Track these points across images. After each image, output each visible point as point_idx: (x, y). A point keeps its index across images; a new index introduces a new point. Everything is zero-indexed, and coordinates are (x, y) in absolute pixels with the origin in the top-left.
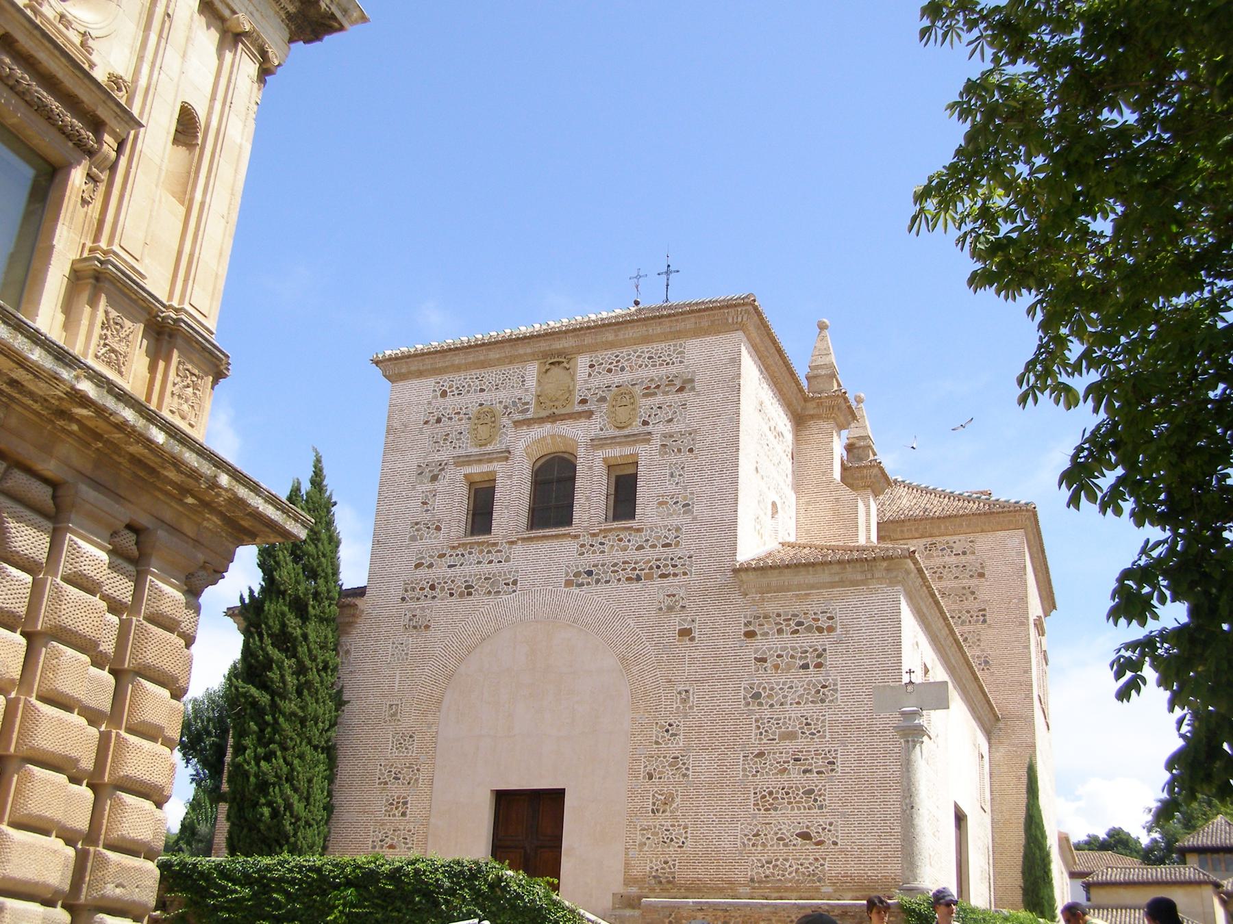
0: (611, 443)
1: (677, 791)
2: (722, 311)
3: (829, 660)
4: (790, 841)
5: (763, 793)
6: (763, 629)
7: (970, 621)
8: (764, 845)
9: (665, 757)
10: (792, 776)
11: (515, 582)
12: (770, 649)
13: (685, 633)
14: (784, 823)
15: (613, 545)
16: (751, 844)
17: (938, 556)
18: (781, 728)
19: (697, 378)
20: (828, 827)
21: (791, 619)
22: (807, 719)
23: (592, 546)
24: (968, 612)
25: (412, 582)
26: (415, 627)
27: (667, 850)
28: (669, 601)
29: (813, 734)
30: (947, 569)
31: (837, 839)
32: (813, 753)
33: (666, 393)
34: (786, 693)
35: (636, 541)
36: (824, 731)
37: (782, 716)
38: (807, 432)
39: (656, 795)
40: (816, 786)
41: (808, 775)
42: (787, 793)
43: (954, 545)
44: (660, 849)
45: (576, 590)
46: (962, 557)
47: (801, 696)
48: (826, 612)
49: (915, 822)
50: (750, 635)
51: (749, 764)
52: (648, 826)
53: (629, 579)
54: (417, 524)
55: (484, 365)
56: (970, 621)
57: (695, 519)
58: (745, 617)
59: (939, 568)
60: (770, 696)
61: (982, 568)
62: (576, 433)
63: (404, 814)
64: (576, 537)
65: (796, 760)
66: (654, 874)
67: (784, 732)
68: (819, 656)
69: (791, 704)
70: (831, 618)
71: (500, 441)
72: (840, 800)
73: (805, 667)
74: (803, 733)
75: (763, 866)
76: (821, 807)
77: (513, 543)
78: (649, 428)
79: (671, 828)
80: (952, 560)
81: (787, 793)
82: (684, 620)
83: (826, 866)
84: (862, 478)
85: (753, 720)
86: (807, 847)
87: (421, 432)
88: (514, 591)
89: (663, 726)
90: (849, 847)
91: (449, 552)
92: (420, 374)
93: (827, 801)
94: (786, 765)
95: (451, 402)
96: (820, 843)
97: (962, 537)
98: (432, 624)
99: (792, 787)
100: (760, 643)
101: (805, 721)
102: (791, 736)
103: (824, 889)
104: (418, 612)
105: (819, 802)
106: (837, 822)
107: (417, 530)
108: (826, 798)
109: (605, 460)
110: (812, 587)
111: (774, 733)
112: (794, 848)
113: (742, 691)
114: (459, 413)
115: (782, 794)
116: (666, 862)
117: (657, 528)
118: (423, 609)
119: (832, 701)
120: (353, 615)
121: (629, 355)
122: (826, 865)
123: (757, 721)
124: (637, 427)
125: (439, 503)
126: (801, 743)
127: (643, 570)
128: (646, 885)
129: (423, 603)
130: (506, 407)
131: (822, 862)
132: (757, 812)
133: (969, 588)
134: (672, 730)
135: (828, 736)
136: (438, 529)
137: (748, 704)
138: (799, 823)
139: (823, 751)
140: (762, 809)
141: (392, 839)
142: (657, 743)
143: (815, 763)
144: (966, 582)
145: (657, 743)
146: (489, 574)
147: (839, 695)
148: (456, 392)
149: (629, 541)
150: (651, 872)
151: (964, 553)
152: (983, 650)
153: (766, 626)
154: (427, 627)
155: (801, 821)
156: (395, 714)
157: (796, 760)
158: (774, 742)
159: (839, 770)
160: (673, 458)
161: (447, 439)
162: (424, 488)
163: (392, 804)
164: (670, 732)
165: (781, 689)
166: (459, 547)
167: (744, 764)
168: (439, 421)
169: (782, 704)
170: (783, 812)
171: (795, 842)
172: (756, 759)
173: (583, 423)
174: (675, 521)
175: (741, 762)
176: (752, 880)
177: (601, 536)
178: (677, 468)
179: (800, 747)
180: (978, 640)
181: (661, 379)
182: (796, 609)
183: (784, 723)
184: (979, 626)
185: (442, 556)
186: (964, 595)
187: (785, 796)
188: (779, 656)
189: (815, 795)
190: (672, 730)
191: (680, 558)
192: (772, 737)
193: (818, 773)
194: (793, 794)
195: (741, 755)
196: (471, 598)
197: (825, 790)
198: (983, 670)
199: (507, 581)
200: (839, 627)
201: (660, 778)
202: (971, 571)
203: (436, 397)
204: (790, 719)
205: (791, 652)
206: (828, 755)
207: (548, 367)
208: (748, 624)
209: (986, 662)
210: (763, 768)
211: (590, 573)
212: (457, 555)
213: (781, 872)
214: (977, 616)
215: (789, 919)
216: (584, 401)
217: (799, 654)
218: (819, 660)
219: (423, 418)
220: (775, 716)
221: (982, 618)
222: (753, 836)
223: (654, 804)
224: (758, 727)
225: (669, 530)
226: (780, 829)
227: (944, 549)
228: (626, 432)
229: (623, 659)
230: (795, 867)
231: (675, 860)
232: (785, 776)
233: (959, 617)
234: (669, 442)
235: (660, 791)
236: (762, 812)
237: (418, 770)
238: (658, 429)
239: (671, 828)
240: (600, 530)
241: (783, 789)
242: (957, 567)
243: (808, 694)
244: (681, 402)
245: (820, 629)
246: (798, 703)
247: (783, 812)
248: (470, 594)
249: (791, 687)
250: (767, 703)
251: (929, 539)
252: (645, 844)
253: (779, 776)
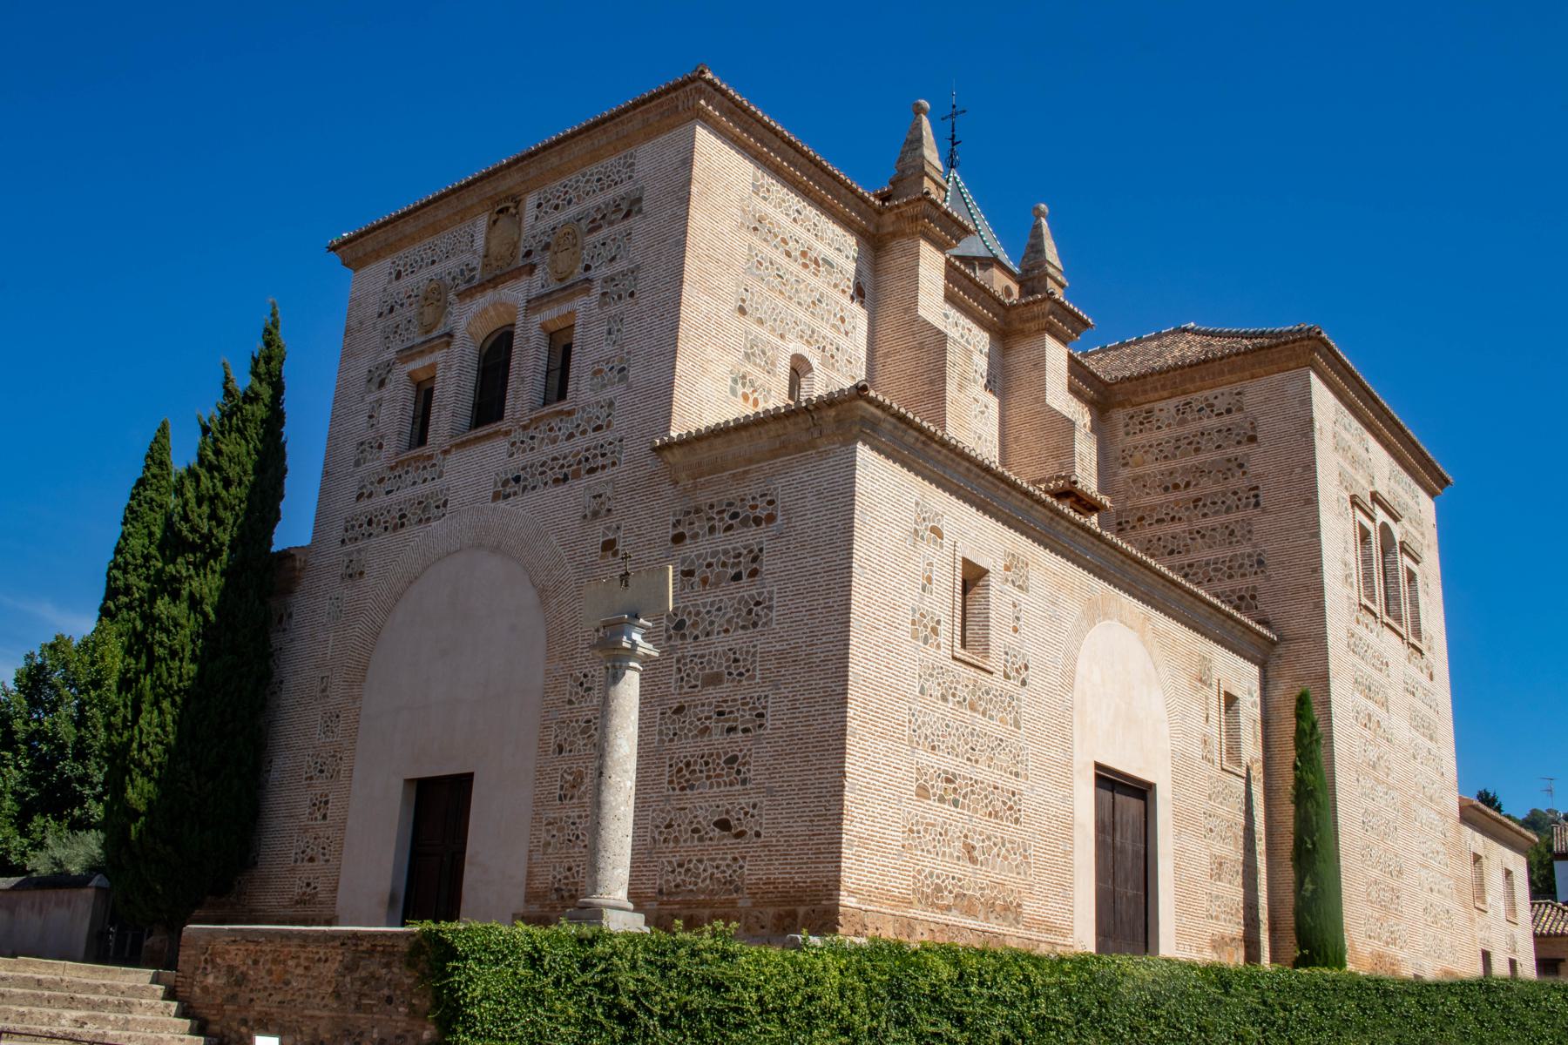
0: (548, 302)
1: (587, 767)
3: (766, 564)
4: (706, 833)
5: (681, 765)
6: (693, 529)
7: (1237, 507)
8: (676, 840)
9: (577, 721)
10: (713, 738)
11: (445, 504)
12: (699, 556)
13: (609, 546)
14: (701, 808)
15: (543, 439)
16: (662, 839)
17: (1194, 420)
18: (704, 668)
19: (646, 194)
20: (751, 810)
21: (723, 511)
22: (735, 653)
23: (522, 442)
24: (1235, 493)
25: (352, 519)
26: (350, 576)
27: (571, 851)
28: (594, 504)
29: (741, 674)
30: (1206, 437)
31: (761, 827)
32: (739, 702)
33: (611, 223)
34: (713, 618)
35: (567, 429)
36: (754, 669)
37: (707, 651)
38: (888, 258)
39: (565, 775)
40: (741, 751)
41: (732, 735)
42: (707, 763)
43: (1215, 402)
44: (564, 851)
45: (502, 504)
46: (1226, 419)
47: (729, 621)
48: (765, 495)
49: (602, 799)
50: (678, 539)
51: (666, 724)
52: (554, 818)
53: (556, 481)
54: (362, 444)
55: (436, 229)
56: (1237, 507)
57: (629, 387)
58: (674, 515)
59: (1194, 436)
60: (695, 624)
61: (1254, 428)
62: (515, 293)
63: (324, 817)
64: (507, 433)
65: (721, 714)
66: (556, 886)
67: (708, 675)
68: (755, 559)
69: (718, 633)
70: (771, 503)
71: (445, 324)
72: (768, 769)
73: (737, 577)
74: (730, 674)
75: (673, 872)
76: (744, 782)
77: (446, 452)
78: (591, 274)
79: (578, 821)
80: (1212, 422)
81: (707, 763)
82: (608, 528)
83: (745, 869)
84: (1033, 318)
85: (674, 660)
86: (725, 841)
87: (375, 328)
88: (444, 515)
89: (577, 679)
90: (774, 839)
91: (387, 474)
92: (377, 255)
93: (752, 772)
94: (708, 722)
95: (407, 282)
96: (741, 835)
97: (1226, 389)
98: (366, 570)
99: (712, 755)
100: (689, 549)
101: (732, 656)
102: (714, 680)
103: (741, 903)
104: (354, 557)
105: (742, 775)
106: (762, 802)
107: (362, 452)
108: (752, 768)
109: (543, 327)
110: (750, 461)
111: (696, 678)
112: (710, 843)
113: (665, 621)
114: (410, 296)
115: (701, 765)
116: (570, 869)
117: (589, 406)
118: (359, 551)
119: (765, 624)
120: (294, 569)
121: (577, 182)
122: (746, 867)
123: (678, 661)
124: (579, 274)
125: (384, 414)
126: (725, 690)
127: (570, 466)
128: (548, 902)
129: (360, 544)
130: (454, 279)
131: (741, 862)
132: (671, 792)
133: (1236, 459)
134: (587, 682)
135: (758, 676)
136: (380, 446)
137: (670, 638)
138: (718, 807)
139: (751, 698)
140: (677, 788)
141: (312, 849)
142: (570, 702)
143: (742, 716)
144: (1231, 452)
145: (570, 702)
147: (774, 614)
148: (410, 270)
149: (560, 429)
150: (553, 883)
151: (1229, 411)
152: (1255, 546)
153: (697, 524)
154: (361, 573)
155: (720, 803)
156: (324, 690)
157: (721, 714)
158: (696, 690)
159: (768, 725)
160: (613, 309)
161: (396, 332)
162: (370, 398)
163: (314, 805)
164: (585, 686)
165: (708, 612)
166: (397, 466)
167: (661, 725)
168: (391, 310)
169: (708, 635)
170: (699, 791)
171: (711, 835)
172: (675, 717)
173: (524, 282)
174: (608, 394)
175: (657, 724)
176: (661, 892)
177: (532, 427)
178: (615, 322)
179: (724, 695)
180: (1250, 532)
181: (607, 205)
182: (732, 494)
183: (709, 662)
184: (1250, 511)
185: (381, 481)
186: (1229, 470)
187: (704, 768)
188: (709, 565)
189: (739, 765)
190: (587, 682)
191: (611, 443)
192: (694, 683)
193: (746, 730)
194: (713, 763)
195: (659, 712)
196: (404, 530)
197: (750, 756)
198: (1256, 573)
200: (779, 514)
201: (570, 751)
202: (1238, 435)
203: (390, 282)
204: (715, 655)
205: (723, 558)
206: (757, 705)
207: (494, 217)
208: (677, 524)
209: (1260, 563)
210: (682, 729)
211: (517, 479)
212: (395, 477)
213: (693, 879)
214: (1247, 498)
215: (317, 957)
216: (528, 254)
217: (732, 560)
218: (754, 566)
219: (377, 310)
220: (699, 653)
221: (1253, 500)
222: (667, 827)
223: (562, 787)
224: (679, 670)
225: (602, 407)
226: (695, 817)
227: (1201, 410)
228: (568, 282)
229: (543, 593)
230: (710, 871)
231: (579, 866)
232: (705, 739)
233: (1223, 502)
234: (610, 288)
235: (570, 768)
236: (677, 792)
237: (341, 759)
238: (600, 272)
239: (578, 821)
240: (531, 420)
241: (702, 757)
242: (1219, 431)
243: (738, 617)
244: (626, 231)
245: (757, 521)
246: (727, 631)
247: (699, 791)
248: (403, 525)
249: (719, 609)
250: (691, 633)
251: (1181, 399)
252: (549, 844)
253: (699, 739)
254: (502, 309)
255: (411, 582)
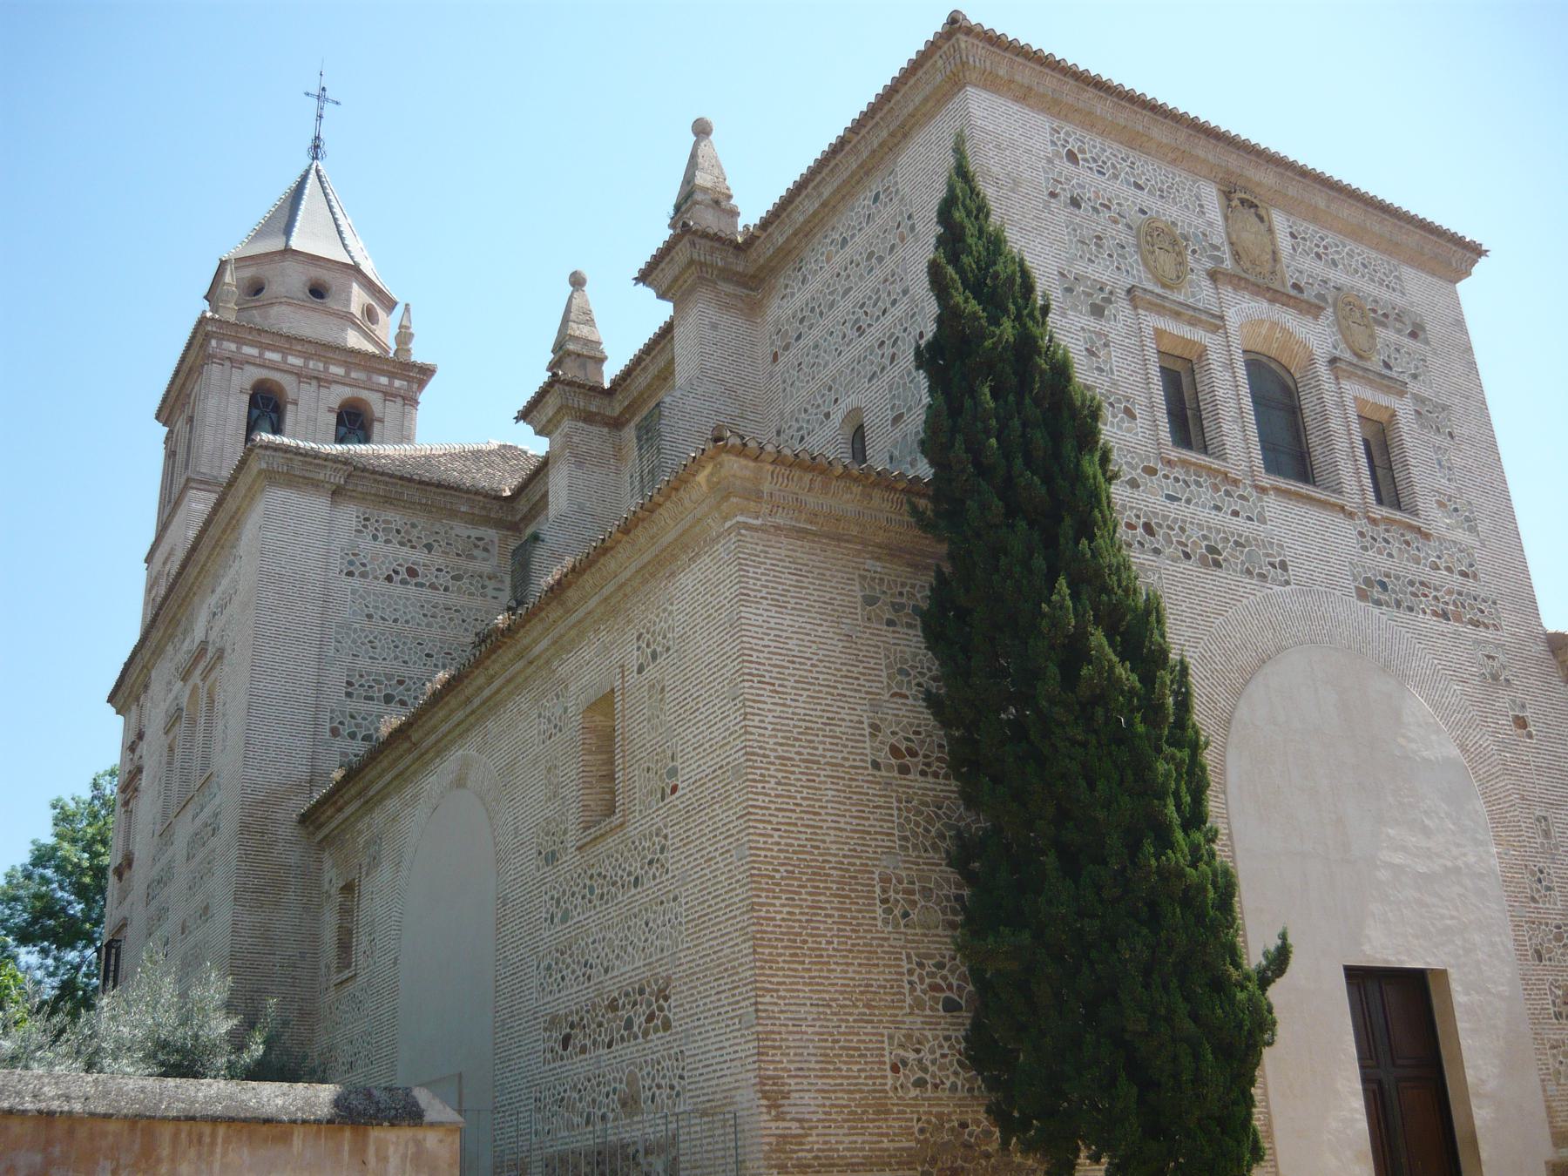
0: (1363, 377)
2: (1449, 245)
9: (1547, 924)
52: (1557, 1040)
55: (1133, 141)
88: (1287, 583)
145: (1533, 899)
146: (1240, 536)
199: (1271, 560)
248: (1217, 564)
254: (1278, 335)
255: (1264, 662)
